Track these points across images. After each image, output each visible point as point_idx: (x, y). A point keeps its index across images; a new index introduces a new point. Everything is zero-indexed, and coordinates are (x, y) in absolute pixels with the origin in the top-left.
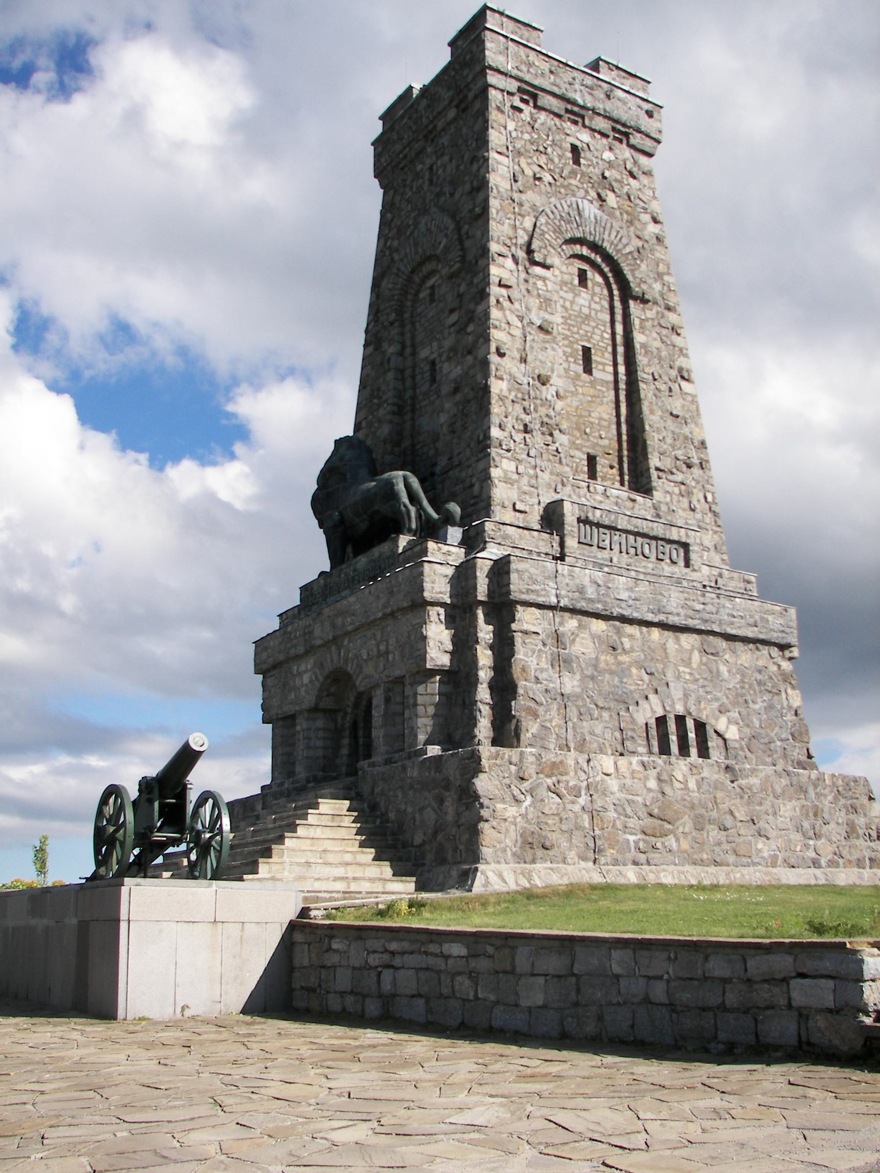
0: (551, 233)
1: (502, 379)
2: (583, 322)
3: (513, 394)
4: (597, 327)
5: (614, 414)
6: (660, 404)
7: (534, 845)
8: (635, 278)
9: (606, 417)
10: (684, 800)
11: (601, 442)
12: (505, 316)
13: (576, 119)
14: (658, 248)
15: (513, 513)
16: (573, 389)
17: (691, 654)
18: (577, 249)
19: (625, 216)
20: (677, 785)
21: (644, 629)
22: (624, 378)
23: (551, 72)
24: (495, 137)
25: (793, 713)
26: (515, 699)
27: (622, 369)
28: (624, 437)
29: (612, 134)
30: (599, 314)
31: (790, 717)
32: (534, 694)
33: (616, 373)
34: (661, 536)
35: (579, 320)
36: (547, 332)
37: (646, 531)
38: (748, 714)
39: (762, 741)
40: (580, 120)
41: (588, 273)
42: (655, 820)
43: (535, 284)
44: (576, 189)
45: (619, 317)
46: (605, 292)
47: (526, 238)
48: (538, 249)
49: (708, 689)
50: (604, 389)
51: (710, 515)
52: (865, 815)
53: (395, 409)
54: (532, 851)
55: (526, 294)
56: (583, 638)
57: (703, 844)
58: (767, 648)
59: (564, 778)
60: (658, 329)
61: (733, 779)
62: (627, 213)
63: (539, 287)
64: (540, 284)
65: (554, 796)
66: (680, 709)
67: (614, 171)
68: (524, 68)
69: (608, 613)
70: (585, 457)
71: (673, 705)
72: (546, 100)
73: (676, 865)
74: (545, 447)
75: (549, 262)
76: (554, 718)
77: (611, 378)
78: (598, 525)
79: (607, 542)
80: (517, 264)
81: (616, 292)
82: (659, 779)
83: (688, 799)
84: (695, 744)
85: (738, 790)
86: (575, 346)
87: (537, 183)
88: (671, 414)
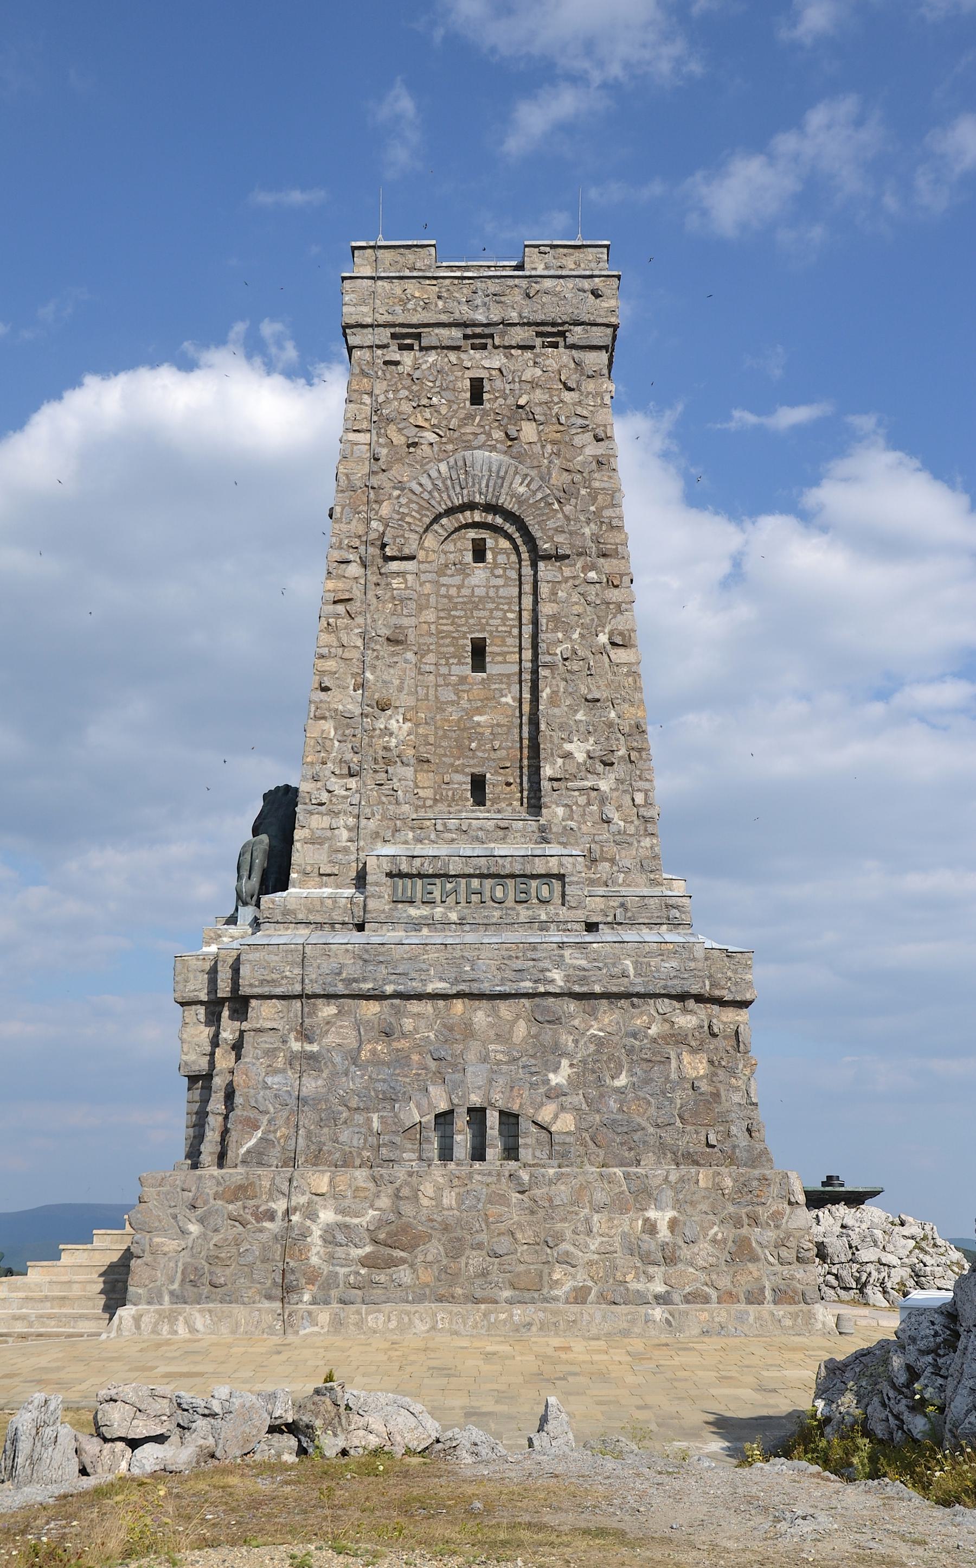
0: (414, 513)
1: (324, 718)
2: (476, 608)
3: (340, 732)
4: (497, 609)
5: (518, 714)
6: (570, 690)
9: (504, 721)
10: (432, 1220)
12: (339, 639)
13: (483, 341)
15: (318, 879)
16: (455, 698)
17: (512, 1027)
18: (467, 517)
19: (549, 447)
20: (425, 1202)
21: (441, 1003)
22: (529, 665)
23: (439, 297)
25: (688, 1086)
26: (233, 1110)
27: (527, 654)
29: (538, 342)
30: (501, 590)
32: (256, 1102)
34: (517, 872)
35: (470, 606)
37: (493, 870)
38: (602, 1096)
40: (489, 341)
44: (471, 437)
45: (527, 588)
46: (514, 558)
48: (390, 541)
49: (533, 1069)
51: (636, 822)
54: (195, 1290)
55: (374, 600)
56: (341, 1027)
57: (456, 1275)
59: (251, 1203)
62: (554, 443)
63: (395, 586)
64: (396, 583)
65: (237, 1224)
66: (475, 1100)
67: (538, 391)
68: (398, 309)
69: (376, 992)
71: (464, 1097)
75: (407, 551)
76: (280, 1127)
78: (420, 876)
79: (437, 894)
80: (365, 567)
81: (525, 556)
82: (397, 1196)
83: (439, 1219)
85: (528, 1203)
86: (461, 642)
87: (412, 450)
88: (587, 700)
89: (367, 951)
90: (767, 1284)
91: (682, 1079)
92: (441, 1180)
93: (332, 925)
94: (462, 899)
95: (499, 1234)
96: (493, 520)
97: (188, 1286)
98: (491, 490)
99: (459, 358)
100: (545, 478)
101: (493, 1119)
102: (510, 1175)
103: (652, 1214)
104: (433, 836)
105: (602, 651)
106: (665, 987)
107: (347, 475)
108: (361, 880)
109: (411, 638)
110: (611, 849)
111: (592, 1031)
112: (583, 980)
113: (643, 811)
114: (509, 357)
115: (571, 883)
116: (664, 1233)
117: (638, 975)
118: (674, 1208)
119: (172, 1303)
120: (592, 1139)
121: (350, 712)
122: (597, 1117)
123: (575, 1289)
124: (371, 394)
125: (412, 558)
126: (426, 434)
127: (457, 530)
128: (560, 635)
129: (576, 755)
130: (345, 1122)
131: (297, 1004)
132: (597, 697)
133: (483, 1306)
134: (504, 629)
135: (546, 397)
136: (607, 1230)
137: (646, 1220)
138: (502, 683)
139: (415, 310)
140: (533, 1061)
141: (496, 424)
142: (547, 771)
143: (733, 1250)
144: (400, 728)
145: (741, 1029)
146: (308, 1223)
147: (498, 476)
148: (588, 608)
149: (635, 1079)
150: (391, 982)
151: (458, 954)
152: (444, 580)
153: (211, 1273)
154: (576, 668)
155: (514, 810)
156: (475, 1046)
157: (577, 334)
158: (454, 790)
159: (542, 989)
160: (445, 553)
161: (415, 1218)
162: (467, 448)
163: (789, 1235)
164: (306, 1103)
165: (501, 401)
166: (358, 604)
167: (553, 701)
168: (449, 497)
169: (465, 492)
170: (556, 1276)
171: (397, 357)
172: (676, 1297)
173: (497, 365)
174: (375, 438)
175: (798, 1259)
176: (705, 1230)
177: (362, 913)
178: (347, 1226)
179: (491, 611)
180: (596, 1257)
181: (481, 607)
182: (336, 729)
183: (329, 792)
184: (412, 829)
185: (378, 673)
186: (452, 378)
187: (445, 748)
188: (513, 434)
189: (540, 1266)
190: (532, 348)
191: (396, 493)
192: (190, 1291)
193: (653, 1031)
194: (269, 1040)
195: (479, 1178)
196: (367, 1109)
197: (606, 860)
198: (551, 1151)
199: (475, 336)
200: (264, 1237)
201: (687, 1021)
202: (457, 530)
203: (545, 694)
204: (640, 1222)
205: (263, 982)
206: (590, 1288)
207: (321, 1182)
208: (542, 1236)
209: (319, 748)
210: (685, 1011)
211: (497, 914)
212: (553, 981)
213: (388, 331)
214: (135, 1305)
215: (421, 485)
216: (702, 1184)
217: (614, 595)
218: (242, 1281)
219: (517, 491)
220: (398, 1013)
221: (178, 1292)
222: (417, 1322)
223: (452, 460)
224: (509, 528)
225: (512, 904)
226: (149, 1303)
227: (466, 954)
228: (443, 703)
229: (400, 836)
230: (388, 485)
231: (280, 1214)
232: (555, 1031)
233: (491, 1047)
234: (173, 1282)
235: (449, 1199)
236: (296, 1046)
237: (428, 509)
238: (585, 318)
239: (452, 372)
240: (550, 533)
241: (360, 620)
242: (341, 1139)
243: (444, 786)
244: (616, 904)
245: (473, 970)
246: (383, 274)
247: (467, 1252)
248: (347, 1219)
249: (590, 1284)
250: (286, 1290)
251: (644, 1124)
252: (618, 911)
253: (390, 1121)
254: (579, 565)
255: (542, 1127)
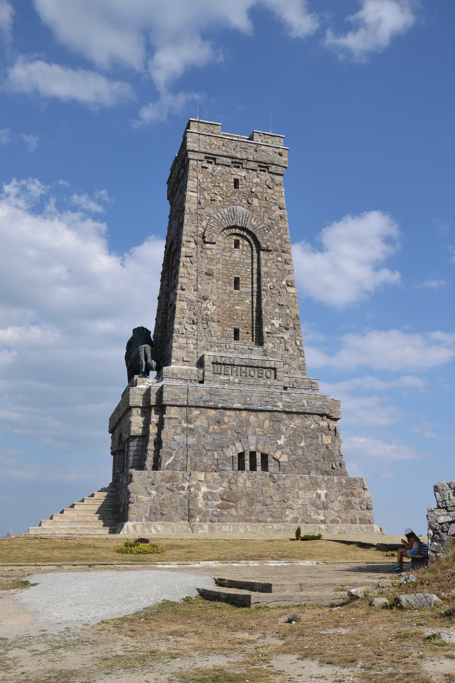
1: (183, 301)
2: (236, 266)
3: (189, 307)
4: (243, 267)
7: (157, 514)
8: (263, 240)
9: (246, 309)
10: (243, 492)
11: (242, 322)
12: (188, 271)
13: (238, 165)
14: (280, 222)
15: (182, 363)
16: (228, 299)
17: (264, 422)
19: (263, 209)
20: (240, 485)
21: (238, 412)
22: (256, 289)
23: (224, 146)
24: (191, 184)
25: (325, 447)
26: (162, 448)
27: (255, 285)
28: (255, 318)
29: (259, 169)
30: (245, 260)
31: (323, 450)
32: (171, 445)
33: (252, 288)
36: (210, 275)
37: (251, 364)
39: (303, 462)
40: (241, 165)
41: (240, 241)
42: (225, 501)
43: (206, 252)
44: (235, 201)
45: (255, 260)
46: (250, 249)
47: (203, 231)
48: (207, 236)
49: (272, 438)
50: (246, 296)
51: (297, 351)
52: (360, 497)
53: (164, 311)
54: (155, 516)
55: (200, 258)
56: (202, 419)
57: (252, 512)
58: (312, 416)
59: (175, 483)
60: (276, 263)
61: (274, 481)
62: (264, 207)
63: (208, 253)
64: (209, 252)
65: (170, 491)
66: (253, 448)
67: (258, 187)
68: (208, 147)
69: (215, 406)
70: (233, 330)
71: (249, 447)
72: (220, 160)
73: (235, 522)
74: (203, 330)
75: (213, 241)
77: (250, 290)
78: (224, 364)
79: (230, 372)
80: (197, 244)
81: (254, 248)
82: (229, 482)
83: (245, 491)
84: (260, 464)
85: (276, 486)
86: (230, 278)
87: (213, 202)
88: (279, 305)
89: (211, 390)
90: (357, 517)
91: (323, 444)
92: (245, 477)
93: (191, 380)
94: (239, 374)
95: (267, 497)
96: (243, 233)
97: (152, 514)
98: (243, 222)
99: (230, 170)
100: (262, 220)
101: (258, 456)
102: (270, 476)
103: (319, 491)
104: (225, 350)
105: (284, 287)
106: (317, 411)
107: (189, 208)
108: (201, 363)
109: (215, 274)
110: (289, 361)
111: (291, 426)
112: (289, 407)
113: (300, 348)
114: (248, 172)
115: (279, 371)
116: (323, 498)
117: (308, 406)
118: (326, 490)
119: (146, 521)
120: (293, 465)
121: (193, 299)
122: (295, 457)
123: (294, 518)
124: (197, 178)
125: (214, 243)
126: (218, 197)
127: (229, 235)
128: (269, 280)
129: (276, 325)
130: (205, 455)
131: (184, 409)
132: (283, 304)
133: (262, 524)
134: (246, 275)
135: (261, 190)
136: (306, 496)
137: (317, 494)
138: (245, 295)
139: (214, 149)
140: (272, 435)
141: (244, 197)
142: (265, 329)
143: (346, 505)
144: (212, 308)
145: (337, 428)
146: (197, 491)
147: (246, 217)
148: (278, 271)
149: (307, 444)
150: (220, 403)
151: (245, 394)
152: (224, 253)
153: (161, 510)
154: (275, 292)
155: (250, 343)
156: (251, 429)
157: (273, 168)
158: (228, 334)
159: (275, 409)
160: (225, 243)
161: (236, 491)
162: (234, 204)
163: (364, 500)
164: (190, 447)
165: (245, 189)
166: (195, 258)
167: (267, 304)
168: (228, 222)
169: (234, 221)
170: (287, 513)
171: (207, 165)
172: (328, 521)
173: (243, 175)
174: (199, 195)
175: (367, 508)
176: (336, 497)
177: (202, 377)
178: (212, 493)
179: (242, 267)
180: (301, 506)
181: (238, 265)
182: (187, 306)
183: (186, 329)
184: (217, 346)
185: (203, 286)
186: (227, 177)
187: (224, 317)
188: (250, 202)
189: (281, 509)
190: (256, 170)
191: (208, 218)
192: (153, 517)
193: (312, 427)
194: (174, 422)
195: (259, 476)
196: (213, 450)
197: (287, 364)
198: (279, 469)
199: (236, 163)
200: (181, 496)
201: (324, 424)
202: (229, 235)
203: (264, 301)
204: (315, 494)
205: (172, 400)
206: (299, 518)
207: (201, 476)
208: (282, 498)
209: (181, 312)
210: (323, 420)
211: (252, 381)
212: (278, 406)
213: (204, 155)
214: (131, 521)
215: (218, 216)
216: (335, 481)
217: (287, 267)
218: (173, 513)
219: (253, 224)
220: (223, 415)
221: (148, 517)
222: (240, 529)
223: (228, 208)
224: (249, 238)
225: (257, 378)
226: (137, 521)
227: (248, 394)
228: (224, 300)
229: (213, 349)
230: (205, 214)
231: (186, 488)
232: (279, 425)
233: (257, 429)
234: (146, 513)
235: (249, 484)
236: (185, 425)
237: (221, 226)
238: (276, 163)
239: (227, 175)
240: (265, 241)
241: (195, 264)
242: (204, 461)
243: (224, 332)
244: (293, 380)
245: (250, 400)
246: (203, 133)
247: (256, 504)
248: (212, 490)
249: (299, 516)
250: (190, 517)
251: (311, 460)
252: (295, 383)
253: (222, 455)
254: (275, 254)
255: (276, 460)
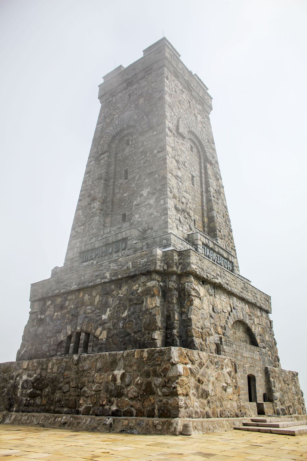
103: (116, 372)
118: (124, 369)
137: (113, 375)
170: (81, 402)
180: (94, 393)
197: (150, 229)
204: (111, 376)
216: (136, 357)
